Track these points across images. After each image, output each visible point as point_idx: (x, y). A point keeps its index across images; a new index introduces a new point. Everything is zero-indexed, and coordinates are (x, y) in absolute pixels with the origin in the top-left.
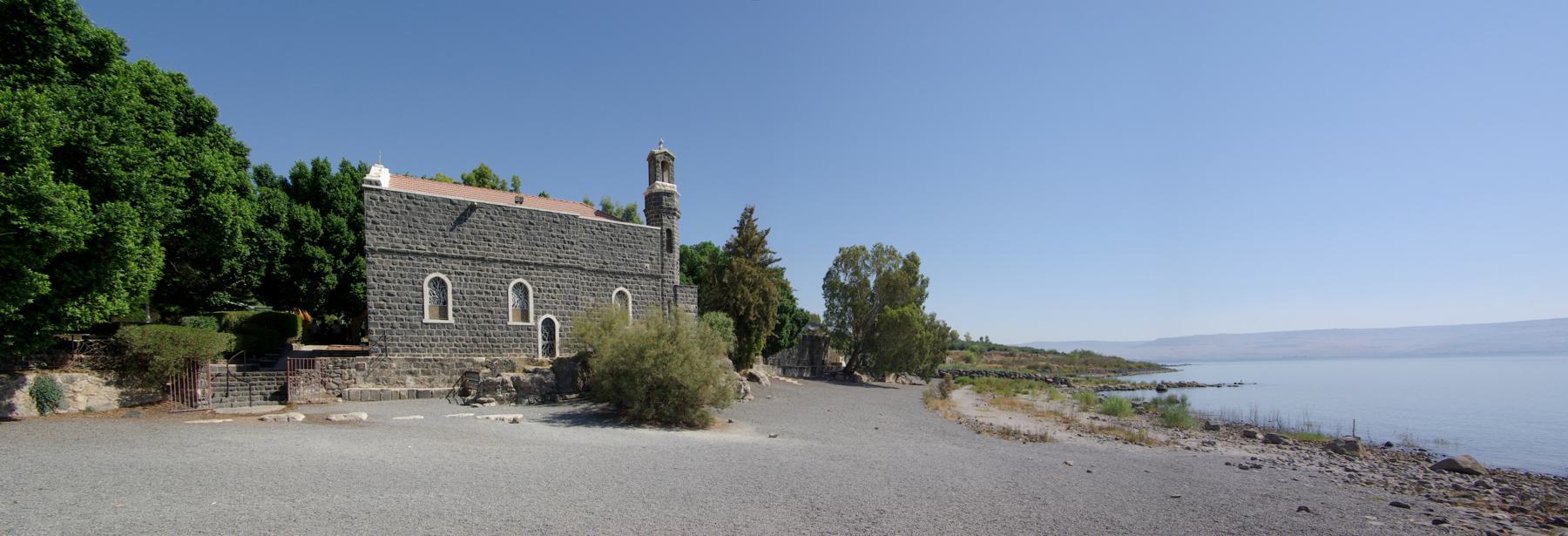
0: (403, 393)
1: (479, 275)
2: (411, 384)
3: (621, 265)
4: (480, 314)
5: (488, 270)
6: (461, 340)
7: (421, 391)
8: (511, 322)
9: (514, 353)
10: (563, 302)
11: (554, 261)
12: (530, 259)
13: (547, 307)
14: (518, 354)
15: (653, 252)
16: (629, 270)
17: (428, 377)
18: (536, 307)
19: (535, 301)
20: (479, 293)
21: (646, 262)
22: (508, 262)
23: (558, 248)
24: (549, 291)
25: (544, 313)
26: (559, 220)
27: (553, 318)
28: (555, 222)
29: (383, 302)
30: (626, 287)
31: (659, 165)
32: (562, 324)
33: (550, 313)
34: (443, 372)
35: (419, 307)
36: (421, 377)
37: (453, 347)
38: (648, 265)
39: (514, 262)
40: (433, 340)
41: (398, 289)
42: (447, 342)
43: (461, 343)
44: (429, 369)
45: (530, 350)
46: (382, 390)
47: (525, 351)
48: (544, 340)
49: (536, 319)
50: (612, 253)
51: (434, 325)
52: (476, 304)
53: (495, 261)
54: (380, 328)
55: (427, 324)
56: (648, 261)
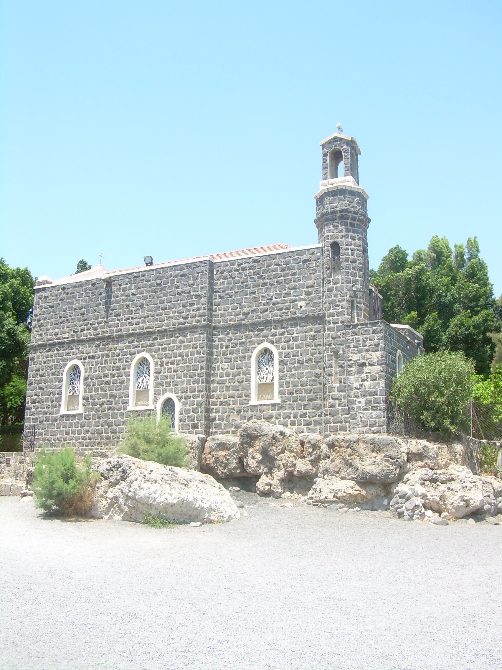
1: (108, 356)
3: (266, 310)
4: (104, 400)
5: (115, 349)
10: (185, 376)
11: (179, 324)
12: (154, 325)
13: (169, 384)
16: (277, 315)
19: (156, 378)
20: (106, 376)
22: (132, 335)
24: (172, 363)
25: (165, 391)
26: (186, 271)
27: (174, 397)
29: (36, 397)
30: (272, 343)
32: (184, 404)
33: (171, 391)
35: (58, 398)
37: (81, 440)
38: (302, 303)
39: (139, 334)
40: (67, 433)
41: (46, 381)
42: (77, 435)
43: (87, 436)
49: (155, 400)
50: (254, 298)
51: (68, 416)
53: (121, 336)
55: (62, 416)
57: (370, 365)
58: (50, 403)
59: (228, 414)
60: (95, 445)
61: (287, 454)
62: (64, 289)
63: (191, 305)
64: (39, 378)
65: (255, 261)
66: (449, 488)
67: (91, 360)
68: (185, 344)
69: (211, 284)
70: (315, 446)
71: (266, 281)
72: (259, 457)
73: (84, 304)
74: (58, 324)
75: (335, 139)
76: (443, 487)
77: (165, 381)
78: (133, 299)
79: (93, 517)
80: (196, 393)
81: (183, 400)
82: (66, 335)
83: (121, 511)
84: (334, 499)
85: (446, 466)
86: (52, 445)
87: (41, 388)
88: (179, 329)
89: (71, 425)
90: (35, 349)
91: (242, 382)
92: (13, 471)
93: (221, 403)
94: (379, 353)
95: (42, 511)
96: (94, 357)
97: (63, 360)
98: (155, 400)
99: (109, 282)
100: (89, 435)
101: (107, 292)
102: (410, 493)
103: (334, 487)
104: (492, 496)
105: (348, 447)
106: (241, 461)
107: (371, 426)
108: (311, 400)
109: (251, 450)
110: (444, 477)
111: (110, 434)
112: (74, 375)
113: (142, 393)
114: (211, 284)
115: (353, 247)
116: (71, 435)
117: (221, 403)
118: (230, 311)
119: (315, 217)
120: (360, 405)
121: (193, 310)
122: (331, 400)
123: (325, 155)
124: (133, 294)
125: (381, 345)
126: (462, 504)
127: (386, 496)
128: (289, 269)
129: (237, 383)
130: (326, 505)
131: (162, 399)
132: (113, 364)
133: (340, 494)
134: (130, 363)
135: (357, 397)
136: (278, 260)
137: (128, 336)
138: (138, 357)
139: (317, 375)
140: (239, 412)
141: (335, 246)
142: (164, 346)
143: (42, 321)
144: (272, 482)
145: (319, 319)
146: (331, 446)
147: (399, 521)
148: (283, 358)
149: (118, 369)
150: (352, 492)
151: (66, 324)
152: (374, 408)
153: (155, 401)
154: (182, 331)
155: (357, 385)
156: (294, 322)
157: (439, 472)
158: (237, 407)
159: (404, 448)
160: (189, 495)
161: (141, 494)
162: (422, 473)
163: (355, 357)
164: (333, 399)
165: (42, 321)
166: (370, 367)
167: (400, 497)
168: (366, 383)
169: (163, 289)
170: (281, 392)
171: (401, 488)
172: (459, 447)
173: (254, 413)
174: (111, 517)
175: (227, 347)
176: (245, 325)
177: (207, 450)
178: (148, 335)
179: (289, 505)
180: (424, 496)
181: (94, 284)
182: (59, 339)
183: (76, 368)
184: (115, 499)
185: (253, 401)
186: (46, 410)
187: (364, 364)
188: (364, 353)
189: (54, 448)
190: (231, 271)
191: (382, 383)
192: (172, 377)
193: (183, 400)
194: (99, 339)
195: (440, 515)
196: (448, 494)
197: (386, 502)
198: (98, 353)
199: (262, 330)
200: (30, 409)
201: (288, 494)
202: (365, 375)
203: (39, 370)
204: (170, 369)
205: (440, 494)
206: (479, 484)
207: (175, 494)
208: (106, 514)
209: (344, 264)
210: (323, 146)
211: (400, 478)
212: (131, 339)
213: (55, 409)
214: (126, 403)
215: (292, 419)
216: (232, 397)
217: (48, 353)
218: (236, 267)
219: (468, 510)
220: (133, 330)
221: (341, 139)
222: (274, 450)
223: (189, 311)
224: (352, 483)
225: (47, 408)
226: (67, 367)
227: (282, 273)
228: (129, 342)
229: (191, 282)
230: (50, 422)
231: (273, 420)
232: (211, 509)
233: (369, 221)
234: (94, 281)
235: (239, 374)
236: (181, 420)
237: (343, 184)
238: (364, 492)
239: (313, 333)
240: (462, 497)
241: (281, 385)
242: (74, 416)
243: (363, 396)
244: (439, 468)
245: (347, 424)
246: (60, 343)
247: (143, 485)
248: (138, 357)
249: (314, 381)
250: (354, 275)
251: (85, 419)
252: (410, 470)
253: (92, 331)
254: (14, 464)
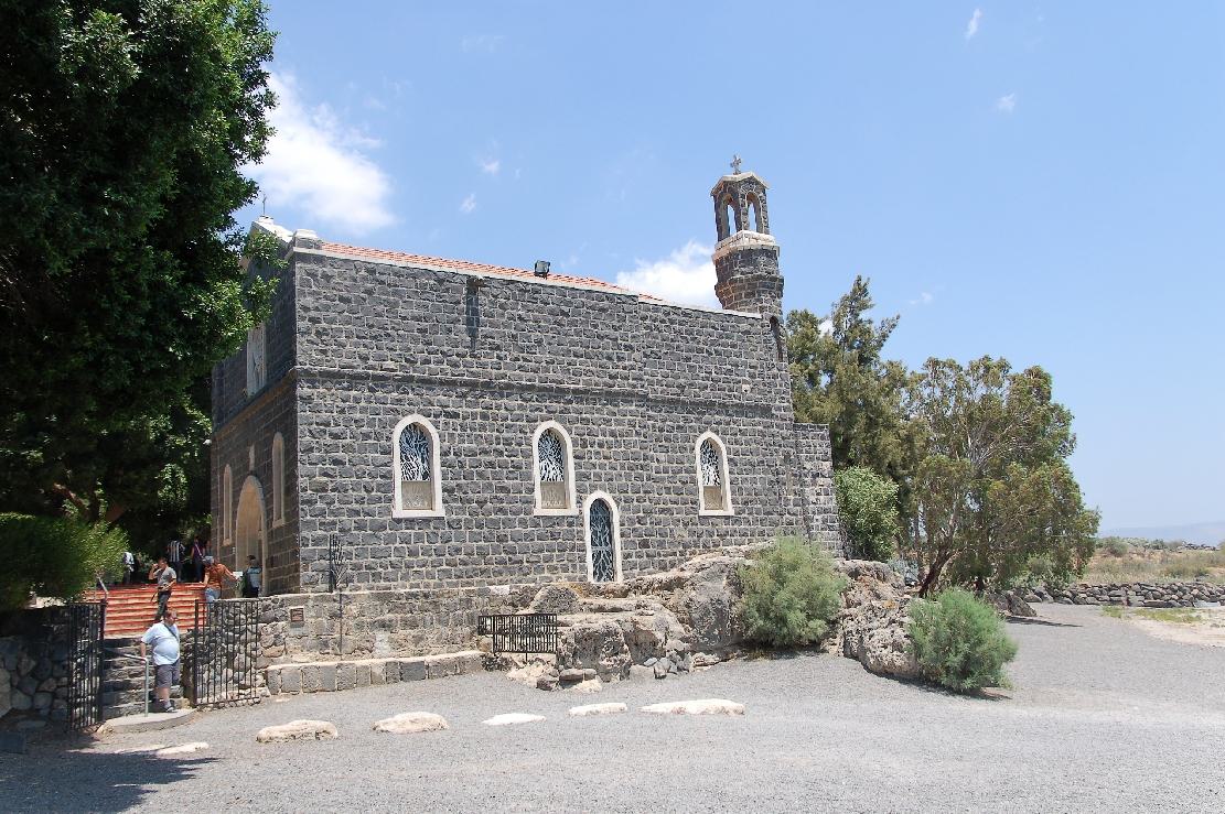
0: (378, 671)
1: (484, 417)
2: (383, 653)
6: (458, 550)
7: (408, 664)
9: (546, 574)
13: (598, 476)
14: (554, 577)
15: (754, 362)
17: (414, 632)
18: (580, 477)
21: (746, 382)
22: (531, 388)
23: (609, 358)
25: (594, 488)
27: (608, 497)
29: (325, 479)
30: (717, 432)
31: (736, 199)
32: (624, 509)
34: (439, 622)
36: (402, 633)
37: (444, 567)
39: (541, 389)
40: (412, 553)
41: (346, 448)
42: (434, 557)
44: (410, 613)
45: (574, 566)
46: (339, 667)
47: (566, 570)
48: (593, 544)
49: (579, 501)
51: (410, 522)
52: (480, 475)
53: (509, 386)
54: (319, 532)
55: (399, 521)
56: (747, 378)
57: (823, 476)
58: (364, 493)
60: (476, 575)
62: (372, 272)
63: (619, 359)
64: (329, 440)
67: (451, 421)
68: (618, 417)
71: (701, 346)
73: (422, 312)
74: (365, 338)
77: (592, 471)
78: (523, 326)
82: (390, 364)
86: (377, 576)
89: (419, 538)
90: (313, 379)
92: (312, 636)
93: (662, 511)
96: (456, 415)
97: (387, 412)
98: (579, 501)
99: (474, 285)
101: (469, 303)
111: (503, 555)
112: (407, 441)
116: (421, 557)
118: (660, 378)
121: (624, 368)
124: (520, 318)
129: (679, 484)
132: (495, 434)
134: (529, 435)
137: (523, 388)
138: (542, 427)
142: (584, 416)
143: (324, 325)
145: (766, 411)
149: (508, 442)
152: (831, 528)
153: (578, 502)
154: (612, 397)
155: (813, 498)
164: (789, 513)
168: (822, 497)
169: (572, 324)
170: (734, 501)
175: (661, 430)
176: (684, 403)
181: (441, 281)
182: (373, 368)
186: (355, 506)
189: (383, 583)
192: (602, 466)
193: (623, 504)
198: (465, 409)
200: (309, 502)
202: (818, 487)
203: (328, 425)
204: (598, 453)
213: (379, 505)
216: (675, 503)
217: (347, 393)
223: (618, 367)
225: (357, 502)
230: (369, 532)
234: (442, 276)
235: (680, 471)
236: (622, 535)
241: (733, 493)
242: (427, 521)
243: (819, 513)
248: (542, 427)
251: (450, 526)
254: (313, 620)
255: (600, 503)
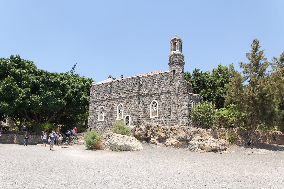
1: (111, 104)
5: (113, 102)
6: (105, 126)
8: (117, 119)
11: (130, 95)
19: (124, 110)
22: (117, 98)
23: (132, 90)
25: (127, 114)
26: (132, 80)
28: (131, 81)
32: (132, 118)
38: (164, 88)
49: (124, 117)
55: (99, 122)
59: (144, 120)
61: (159, 132)
65: (152, 76)
66: (206, 142)
69: (139, 83)
70: (166, 130)
72: (151, 133)
75: (174, 39)
76: (204, 142)
79: (101, 149)
80: (135, 115)
81: (131, 117)
82: (100, 99)
83: (109, 147)
84: (171, 145)
85: (206, 135)
87: (92, 114)
88: (130, 96)
90: (91, 103)
91: (148, 111)
93: (142, 118)
94: (186, 102)
95: (87, 148)
98: (124, 117)
100: (106, 127)
101: (110, 86)
102: (194, 143)
103: (172, 141)
104: (220, 145)
105: (176, 130)
106: (146, 134)
107: (184, 124)
108: (167, 116)
109: (148, 131)
110: (204, 139)
113: (120, 114)
114: (139, 83)
115: (179, 71)
117: (142, 118)
119: (169, 62)
120: (181, 117)
122: (172, 116)
123: (171, 44)
125: (187, 100)
126: (210, 147)
127: (187, 144)
128: (161, 78)
129: (146, 112)
130: (169, 146)
131: (126, 116)
133: (173, 143)
135: (180, 115)
136: (158, 76)
138: (119, 104)
139: (169, 109)
140: (147, 120)
141: (174, 71)
144: (154, 140)
145: (169, 93)
146: (171, 129)
147: (191, 152)
148: (159, 104)
149: (114, 108)
150: (176, 143)
151: (99, 96)
152: (185, 119)
154: (131, 97)
155: (180, 112)
156: (162, 94)
157: (203, 137)
158: (146, 118)
159: (193, 130)
160: (128, 143)
161: (114, 143)
162: (197, 138)
163: (179, 104)
165: (93, 95)
166: (184, 107)
167: (191, 145)
171: (191, 142)
172: (210, 130)
173: (151, 120)
174: (106, 149)
177: (136, 131)
178: (122, 98)
179: (159, 146)
180: (198, 144)
182: (97, 100)
183: (102, 108)
184: (107, 144)
185: (151, 117)
187: (182, 106)
188: (182, 102)
190: (145, 79)
191: (187, 111)
193: (131, 117)
194: (108, 100)
195: (203, 150)
196: (206, 144)
197: (187, 146)
199: (153, 96)
201: (159, 143)
205: (203, 144)
206: (215, 141)
207: (123, 143)
208: (105, 148)
209: (176, 76)
210: (171, 41)
211: (191, 139)
212: (117, 99)
214: (116, 118)
215: (162, 122)
218: (146, 78)
219: (212, 149)
220: (118, 97)
221: (176, 39)
222: (155, 131)
224: (177, 140)
226: (100, 108)
227: (159, 80)
228: (117, 100)
229: (133, 83)
231: (157, 122)
232: (134, 147)
233: (185, 63)
235: (147, 109)
237: (176, 53)
238: (180, 143)
239: (167, 97)
240: (210, 145)
242: (102, 122)
244: (203, 136)
245: (177, 123)
246: (97, 101)
247: (114, 140)
249: (168, 111)
250: (180, 79)
252: (194, 136)
253: (106, 97)
255: (128, 117)
